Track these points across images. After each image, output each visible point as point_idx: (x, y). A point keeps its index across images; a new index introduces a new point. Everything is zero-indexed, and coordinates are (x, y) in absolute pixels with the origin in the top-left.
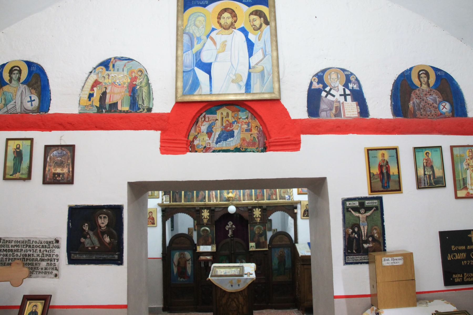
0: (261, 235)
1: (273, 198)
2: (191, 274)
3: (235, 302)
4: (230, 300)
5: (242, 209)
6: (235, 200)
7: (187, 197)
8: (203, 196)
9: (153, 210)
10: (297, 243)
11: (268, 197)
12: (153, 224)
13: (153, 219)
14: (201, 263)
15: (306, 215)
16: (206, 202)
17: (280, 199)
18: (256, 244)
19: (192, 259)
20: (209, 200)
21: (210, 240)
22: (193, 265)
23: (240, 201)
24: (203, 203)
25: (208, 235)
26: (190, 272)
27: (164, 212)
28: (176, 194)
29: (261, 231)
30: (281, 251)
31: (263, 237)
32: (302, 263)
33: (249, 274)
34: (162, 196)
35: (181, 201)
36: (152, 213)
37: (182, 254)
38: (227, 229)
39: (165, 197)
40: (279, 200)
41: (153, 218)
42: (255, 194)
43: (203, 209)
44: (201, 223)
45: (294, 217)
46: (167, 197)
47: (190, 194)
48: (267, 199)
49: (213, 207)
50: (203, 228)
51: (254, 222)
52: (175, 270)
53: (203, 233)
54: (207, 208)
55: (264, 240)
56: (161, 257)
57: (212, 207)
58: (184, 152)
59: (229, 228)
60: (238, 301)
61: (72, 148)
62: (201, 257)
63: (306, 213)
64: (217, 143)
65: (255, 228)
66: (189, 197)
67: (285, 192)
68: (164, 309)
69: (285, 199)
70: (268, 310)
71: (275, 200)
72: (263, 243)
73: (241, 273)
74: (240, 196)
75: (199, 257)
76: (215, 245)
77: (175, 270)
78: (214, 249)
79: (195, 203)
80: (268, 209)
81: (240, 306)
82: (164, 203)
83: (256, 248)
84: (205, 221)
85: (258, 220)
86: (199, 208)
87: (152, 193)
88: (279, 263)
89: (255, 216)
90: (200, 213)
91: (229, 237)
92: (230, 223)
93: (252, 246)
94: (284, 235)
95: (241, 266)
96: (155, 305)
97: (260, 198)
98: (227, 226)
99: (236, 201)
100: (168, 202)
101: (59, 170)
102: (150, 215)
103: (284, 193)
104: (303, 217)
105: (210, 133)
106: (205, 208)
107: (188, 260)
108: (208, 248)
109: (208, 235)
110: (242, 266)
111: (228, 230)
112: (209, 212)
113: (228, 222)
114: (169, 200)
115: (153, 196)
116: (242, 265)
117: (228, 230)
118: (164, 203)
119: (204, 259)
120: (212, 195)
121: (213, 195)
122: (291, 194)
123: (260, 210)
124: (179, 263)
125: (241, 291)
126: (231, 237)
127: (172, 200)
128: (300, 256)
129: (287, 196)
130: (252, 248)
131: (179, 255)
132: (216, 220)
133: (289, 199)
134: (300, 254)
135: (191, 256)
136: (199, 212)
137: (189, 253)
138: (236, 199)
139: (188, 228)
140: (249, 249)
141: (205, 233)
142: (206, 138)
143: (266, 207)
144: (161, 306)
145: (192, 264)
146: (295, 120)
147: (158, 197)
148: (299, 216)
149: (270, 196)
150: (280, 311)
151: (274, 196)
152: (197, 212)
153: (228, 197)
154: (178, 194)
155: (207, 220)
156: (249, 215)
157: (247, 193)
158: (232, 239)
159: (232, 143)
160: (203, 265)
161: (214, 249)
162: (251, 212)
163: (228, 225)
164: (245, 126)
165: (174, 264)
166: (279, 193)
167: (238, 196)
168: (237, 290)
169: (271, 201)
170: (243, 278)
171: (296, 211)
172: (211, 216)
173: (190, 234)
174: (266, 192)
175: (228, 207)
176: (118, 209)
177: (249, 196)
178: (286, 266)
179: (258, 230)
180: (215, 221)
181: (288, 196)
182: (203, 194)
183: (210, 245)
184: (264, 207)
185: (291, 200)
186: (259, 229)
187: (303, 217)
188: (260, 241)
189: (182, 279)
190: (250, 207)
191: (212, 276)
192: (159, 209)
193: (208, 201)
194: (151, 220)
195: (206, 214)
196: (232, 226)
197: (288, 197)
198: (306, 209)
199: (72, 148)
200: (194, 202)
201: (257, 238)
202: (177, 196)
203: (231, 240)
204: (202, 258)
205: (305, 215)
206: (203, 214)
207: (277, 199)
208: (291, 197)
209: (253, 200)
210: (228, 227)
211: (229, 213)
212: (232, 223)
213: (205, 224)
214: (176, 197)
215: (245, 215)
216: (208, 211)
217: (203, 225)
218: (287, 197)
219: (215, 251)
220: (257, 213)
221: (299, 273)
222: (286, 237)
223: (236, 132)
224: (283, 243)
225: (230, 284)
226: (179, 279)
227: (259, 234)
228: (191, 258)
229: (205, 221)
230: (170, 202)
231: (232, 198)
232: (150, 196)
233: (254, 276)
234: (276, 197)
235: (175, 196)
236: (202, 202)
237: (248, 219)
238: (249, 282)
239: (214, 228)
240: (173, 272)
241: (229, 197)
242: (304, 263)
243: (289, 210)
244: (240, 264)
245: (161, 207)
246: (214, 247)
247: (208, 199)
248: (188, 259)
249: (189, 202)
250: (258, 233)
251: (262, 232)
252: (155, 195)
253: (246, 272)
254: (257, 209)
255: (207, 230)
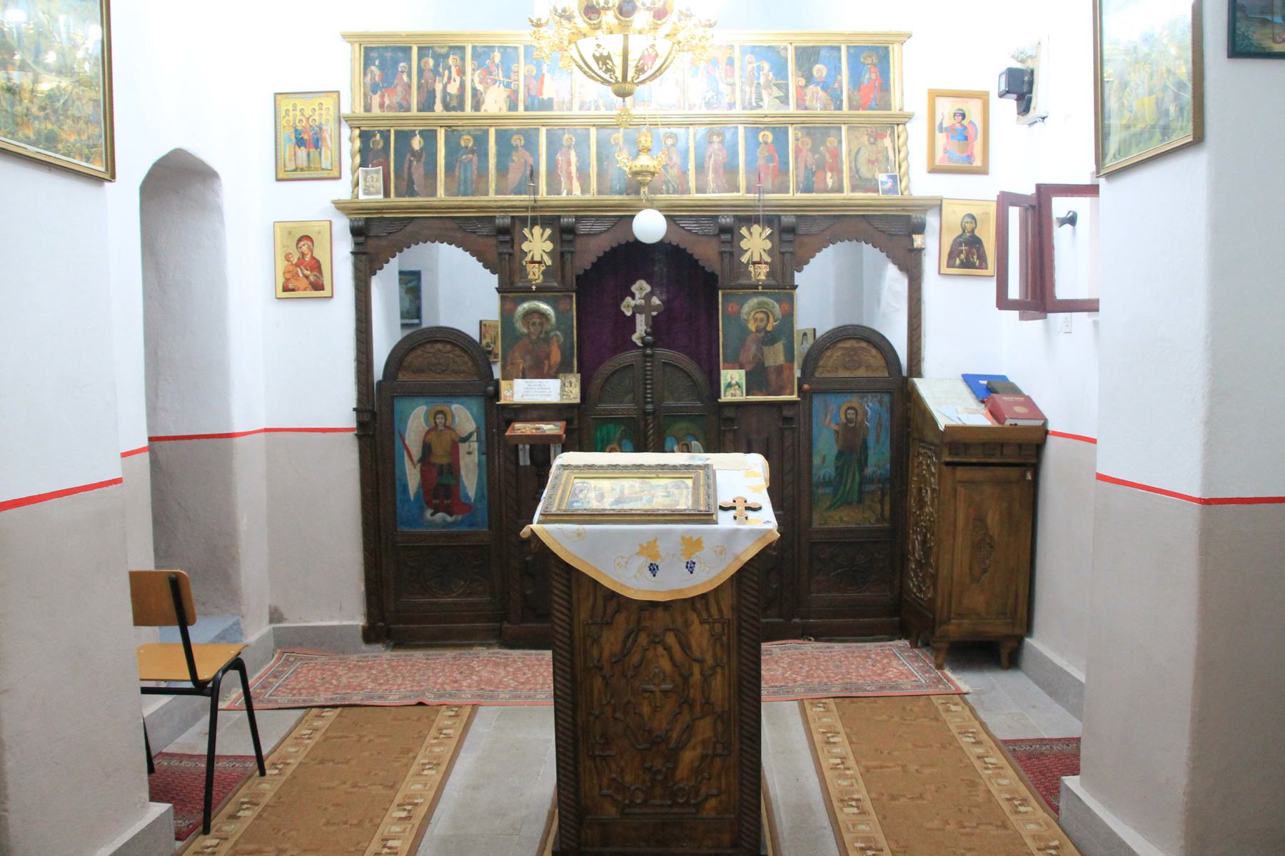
0: (769, 339)
1: (826, 183)
2: (476, 494)
3: (667, 649)
4: (643, 639)
5: (692, 226)
6: (664, 187)
7: (457, 170)
8: (525, 170)
9: (317, 228)
10: (919, 375)
11: (801, 179)
12: (318, 286)
13: (316, 266)
14: (517, 446)
15: (962, 261)
16: (539, 197)
17: (854, 188)
18: (747, 374)
19: (483, 432)
20: (553, 187)
21: (556, 357)
22: (484, 458)
23: (687, 191)
24: (524, 199)
25: (547, 333)
26: (474, 486)
27: (361, 239)
28: (411, 162)
29: (771, 319)
30: (849, 408)
31: (780, 346)
32: (948, 459)
33: (740, 507)
34: (354, 171)
35: (433, 193)
36: (310, 243)
37: (442, 412)
38: (629, 313)
39: (366, 172)
40: (847, 194)
41: (318, 262)
42: (747, 163)
43: (526, 227)
44: (520, 284)
45: (911, 265)
46: (375, 176)
47: (471, 160)
48: (801, 185)
49: (570, 217)
50: (526, 305)
51: (744, 281)
52: (413, 477)
53: (528, 328)
54: (546, 222)
55: (781, 359)
56: (354, 425)
57: (565, 216)
59: (637, 309)
60: (685, 647)
62: (517, 425)
63: (961, 252)
65: (746, 308)
66: (469, 175)
67: (877, 160)
68: (372, 634)
69: (878, 191)
70: (790, 643)
71: (832, 191)
72: (780, 369)
73: (702, 501)
74: (685, 173)
75: (508, 423)
76: (579, 375)
77: (413, 477)
78: (574, 395)
79: (492, 197)
80: (802, 230)
81: (696, 669)
82: (362, 197)
83: (747, 394)
84: (535, 274)
85: (761, 273)
86: (508, 221)
87: (308, 155)
88: (840, 454)
89: (744, 259)
90: (512, 240)
91: (635, 344)
92: (641, 288)
93: (734, 382)
94: (868, 341)
95: (699, 467)
96: (332, 618)
97: (770, 181)
98: (629, 299)
99: (668, 193)
100: (377, 193)
102: (305, 249)
103: (871, 162)
104: (948, 267)
106: (534, 221)
107: (465, 440)
108: (548, 391)
109: (547, 333)
110: (706, 467)
111: (634, 315)
112: (551, 238)
113: (634, 283)
114: (380, 184)
115: (316, 169)
116: (700, 459)
117: (634, 315)
118: (362, 197)
119: (529, 433)
120: (565, 167)
121: (569, 164)
122: (903, 169)
123: (768, 231)
124: (427, 448)
125: (703, 596)
126: (646, 345)
127: (396, 187)
128: (942, 428)
129: (882, 177)
130: (731, 391)
131: (427, 415)
132: (581, 272)
133: (893, 190)
134: (942, 423)
135: (476, 422)
136: (507, 238)
137: (468, 409)
138: (667, 183)
139: (481, 322)
140: (719, 397)
141: (534, 324)
143: (793, 220)
144: (359, 621)
145: (480, 453)
147: (336, 174)
148: (930, 265)
149: (814, 174)
150: (838, 647)
151: (829, 175)
152: (501, 238)
153: (634, 169)
154: (419, 161)
155: (543, 268)
156: (722, 253)
157: (715, 161)
158: (649, 351)
160: (525, 460)
161: (574, 395)
162: (731, 242)
163: (633, 296)
165: (406, 454)
166: (850, 162)
167: (674, 172)
168: (679, 591)
169: (814, 195)
170: (716, 531)
171: (918, 240)
172: (562, 254)
173: (488, 345)
174: (796, 158)
175: (633, 217)
177: (721, 171)
178: (869, 470)
179: (760, 316)
180: (578, 277)
181: (890, 177)
182: (526, 162)
183: (555, 377)
184: (788, 220)
185: (902, 194)
186: (764, 312)
187: (948, 267)
188: (764, 364)
189: (440, 515)
190: (728, 220)
191: (548, 518)
192: (342, 226)
193: (549, 193)
194: (307, 273)
195: (538, 244)
196: (648, 297)
197: (889, 184)
198: (960, 236)
200: (487, 194)
201: (753, 349)
202: (418, 172)
203: (646, 356)
204: (522, 428)
205: (958, 261)
206: (525, 246)
207: (840, 190)
208: (901, 181)
209: (738, 191)
210: (633, 303)
211: (637, 243)
212: (648, 288)
213: (534, 287)
214: (410, 175)
215: (707, 253)
216: (548, 232)
217: (528, 293)
218: (882, 183)
219: (578, 401)
220: (756, 243)
221: (928, 499)
222: (874, 351)
224: (861, 373)
225: (644, 561)
226: (429, 512)
227: (762, 334)
228: (478, 429)
229: (535, 274)
230: (387, 194)
231: (653, 174)
232: (302, 170)
233: (766, 521)
234: (836, 178)
235: (410, 168)
236: (520, 193)
237: (718, 272)
238: (748, 551)
239: (574, 306)
240: (405, 488)
241: (637, 169)
242: (957, 459)
243: (890, 235)
244: (693, 458)
245: (347, 214)
246: (571, 382)
247: (549, 185)
248: (464, 435)
249: (465, 194)
250: (757, 330)
251: (775, 328)
252: (324, 167)
253: (724, 498)
254: (756, 229)
255: (542, 315)
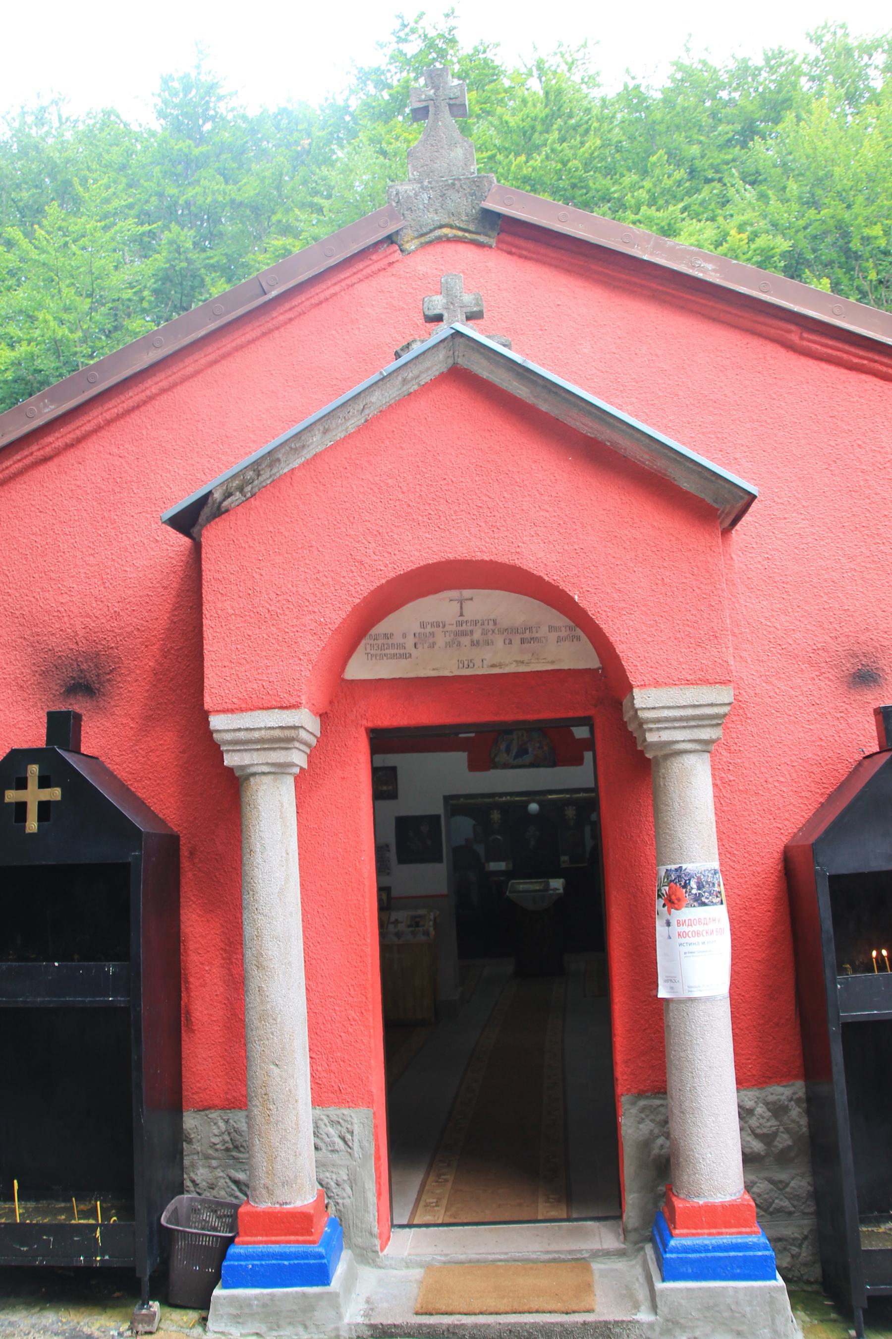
58: (487, 769)
61: (394, 769)
64: (514, 759)
101: (385, 788)
105: (508, 751)
108: (501, 866)
142: (505, 755)
146: (579, 740)
159: (527, 759)
164: (537, 745)
176: (437, 818)
191: (510, 892)
195: (496, 816)
199: (394, 769)
206: (492, 816)
220: (571, 812)
223: (530, 750)
233: (561, 891)
